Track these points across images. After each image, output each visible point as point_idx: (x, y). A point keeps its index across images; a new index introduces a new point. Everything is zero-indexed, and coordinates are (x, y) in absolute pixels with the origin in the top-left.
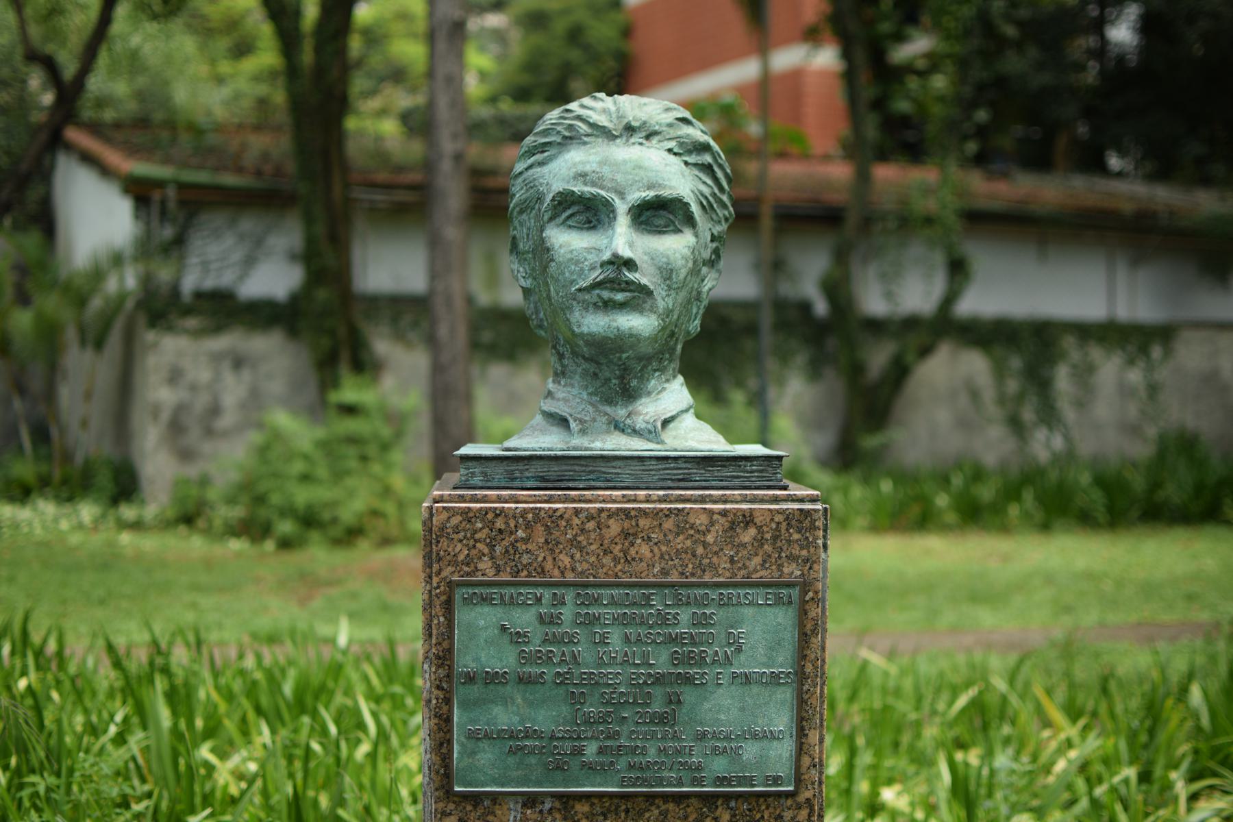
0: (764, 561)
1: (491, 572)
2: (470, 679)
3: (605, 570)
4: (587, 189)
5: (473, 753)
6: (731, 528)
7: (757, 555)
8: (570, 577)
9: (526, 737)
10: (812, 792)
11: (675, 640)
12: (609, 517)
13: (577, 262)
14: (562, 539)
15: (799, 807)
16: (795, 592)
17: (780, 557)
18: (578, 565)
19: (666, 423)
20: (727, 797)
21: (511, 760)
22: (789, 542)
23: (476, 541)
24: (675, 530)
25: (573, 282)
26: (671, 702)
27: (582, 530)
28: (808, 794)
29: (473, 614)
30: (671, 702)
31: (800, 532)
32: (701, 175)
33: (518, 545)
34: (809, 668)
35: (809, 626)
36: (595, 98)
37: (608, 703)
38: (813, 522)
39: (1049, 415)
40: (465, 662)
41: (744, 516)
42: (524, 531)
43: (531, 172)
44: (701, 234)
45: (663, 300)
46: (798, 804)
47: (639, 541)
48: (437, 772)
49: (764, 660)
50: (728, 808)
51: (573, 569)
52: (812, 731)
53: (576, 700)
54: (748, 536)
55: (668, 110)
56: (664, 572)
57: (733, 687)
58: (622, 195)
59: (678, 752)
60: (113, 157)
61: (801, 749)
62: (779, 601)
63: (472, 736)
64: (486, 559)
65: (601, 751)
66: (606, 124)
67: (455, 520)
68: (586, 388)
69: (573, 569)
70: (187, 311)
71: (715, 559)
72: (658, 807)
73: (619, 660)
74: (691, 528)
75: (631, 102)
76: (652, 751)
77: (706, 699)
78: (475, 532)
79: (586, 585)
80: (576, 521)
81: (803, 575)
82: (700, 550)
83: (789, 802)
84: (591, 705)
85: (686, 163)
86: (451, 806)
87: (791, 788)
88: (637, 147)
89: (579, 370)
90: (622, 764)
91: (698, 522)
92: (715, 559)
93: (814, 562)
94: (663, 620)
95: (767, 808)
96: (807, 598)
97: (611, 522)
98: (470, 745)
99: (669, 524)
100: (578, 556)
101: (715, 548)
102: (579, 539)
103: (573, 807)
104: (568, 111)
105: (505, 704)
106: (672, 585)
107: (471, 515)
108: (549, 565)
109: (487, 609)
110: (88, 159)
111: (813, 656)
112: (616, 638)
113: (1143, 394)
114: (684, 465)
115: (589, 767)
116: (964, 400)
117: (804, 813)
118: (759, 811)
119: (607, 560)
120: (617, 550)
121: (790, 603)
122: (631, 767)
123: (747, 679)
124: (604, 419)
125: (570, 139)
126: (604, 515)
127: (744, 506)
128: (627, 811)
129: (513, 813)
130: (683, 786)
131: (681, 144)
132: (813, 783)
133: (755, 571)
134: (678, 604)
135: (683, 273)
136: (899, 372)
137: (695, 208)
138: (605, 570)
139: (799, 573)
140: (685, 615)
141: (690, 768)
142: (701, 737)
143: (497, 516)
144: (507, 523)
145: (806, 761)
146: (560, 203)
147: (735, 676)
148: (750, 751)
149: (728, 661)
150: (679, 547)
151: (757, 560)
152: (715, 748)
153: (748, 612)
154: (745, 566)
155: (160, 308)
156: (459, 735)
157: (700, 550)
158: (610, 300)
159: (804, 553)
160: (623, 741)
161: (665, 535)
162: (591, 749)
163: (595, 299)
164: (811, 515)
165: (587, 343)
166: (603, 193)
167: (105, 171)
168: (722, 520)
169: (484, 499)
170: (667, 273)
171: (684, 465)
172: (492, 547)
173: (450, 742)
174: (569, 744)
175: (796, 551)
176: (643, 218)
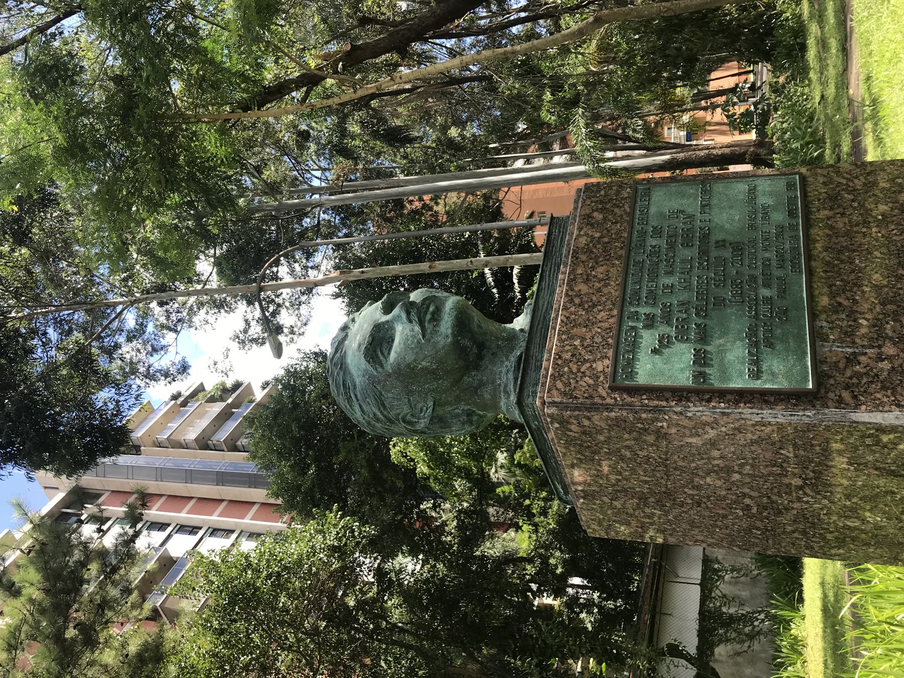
1: (607, 362)
2: (700, 376)
5: (773, 374)
6: (592, 225)
8: (615, 312)
9: (756, 336)
11: (672, 246)
13: (407, 339)
21: (779, 347)
23: (579, 370)
27: (580, 305)
29: (640, 372)
33: (586, 344)
39: (747, 619)
40: (684, 378)
42: (576, 340)
49: (691, 199)
51: (611, 310)
53: (720, 303)
56: (619, 258)
63: (756, 375)
64: (594, 366)
65: (767, 285)
67: (559, 385)
68: (502, 362)
78: (571, 371)
80: (573, 309)
84: (727, 294)
86: (831, 395)
87: (797, 177)
89: (490, 367)
97: (576, 289)
102: (586, 306)
105: (725, 351)
107: (557, 374)
113: (735, 574)
116: (739, 659)
121: (649, 189)
134: (642, 245)
140: (652, 242)
142: (752, 227)
143: (560, 357)
144: (567, 352)
146: (373, 358)
149: (691, 217)
151: (617, 210)
153: (653, 210)
159: (614, 188)
162: (765, 292)
163: (431, 326)
168: (585, 229)
172: (586, 361)
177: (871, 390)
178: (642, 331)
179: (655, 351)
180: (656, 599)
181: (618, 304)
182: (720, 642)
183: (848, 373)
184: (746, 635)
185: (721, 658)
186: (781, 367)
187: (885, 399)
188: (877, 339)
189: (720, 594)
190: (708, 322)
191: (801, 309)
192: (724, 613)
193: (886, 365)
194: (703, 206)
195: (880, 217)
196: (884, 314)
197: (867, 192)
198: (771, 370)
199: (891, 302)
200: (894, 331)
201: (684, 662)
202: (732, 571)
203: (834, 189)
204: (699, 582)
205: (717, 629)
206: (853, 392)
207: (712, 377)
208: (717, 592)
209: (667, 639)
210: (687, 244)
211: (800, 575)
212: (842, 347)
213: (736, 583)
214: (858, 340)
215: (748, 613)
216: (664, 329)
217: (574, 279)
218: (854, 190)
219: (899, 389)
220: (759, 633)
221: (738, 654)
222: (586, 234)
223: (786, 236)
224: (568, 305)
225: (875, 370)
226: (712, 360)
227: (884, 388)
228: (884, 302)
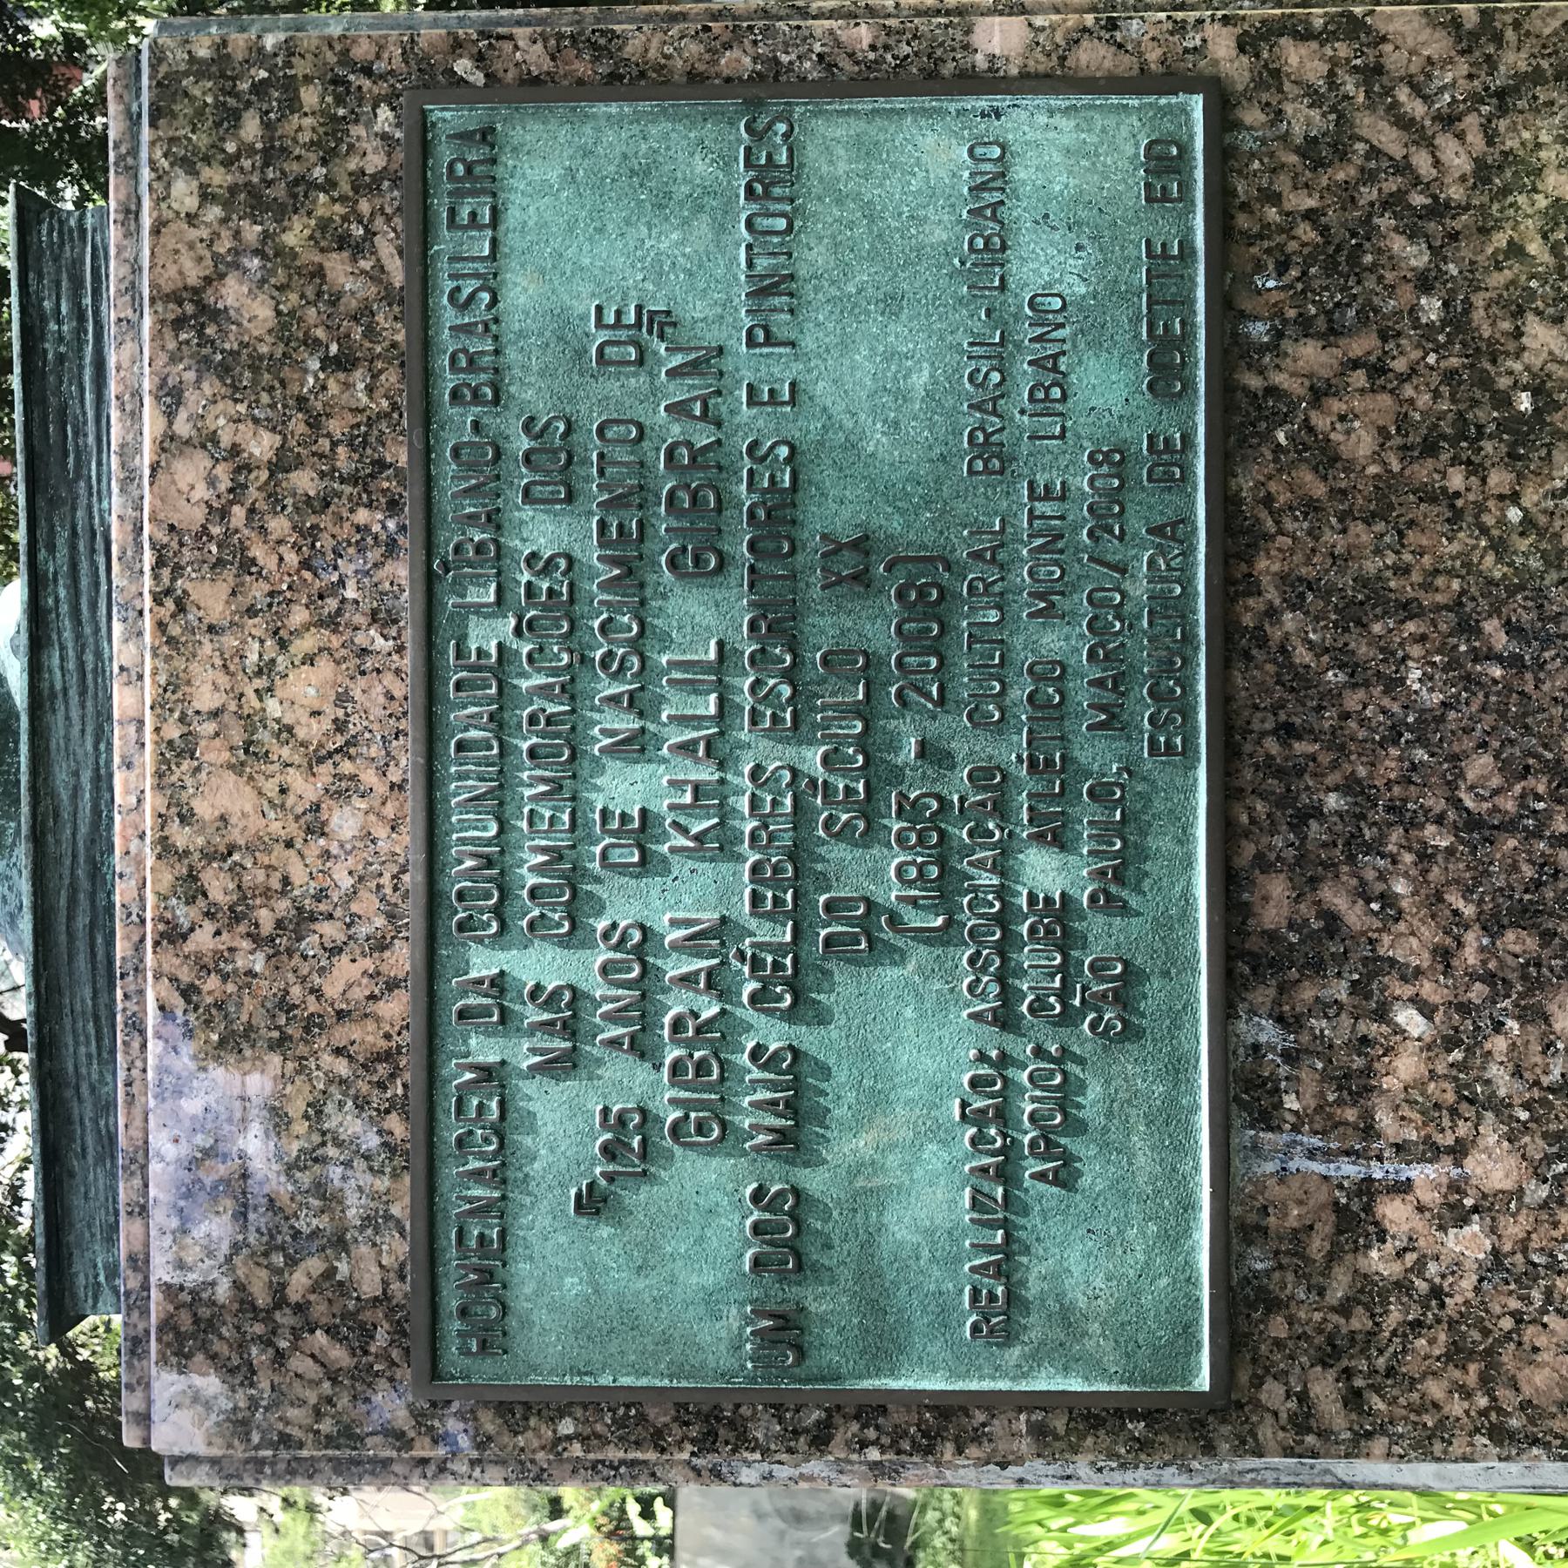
0: (343, 242)
2: (785, 1330)
3: (381, 832)
5: (1067, 1317)
6: (224, 371)
7: (319, 273)
8: (402, 958)
9: (1003, 1116)
10: (1210, 30)
12: (186, 818)
15: (1270, 77)
16: (447, 117)
17: (329, 184)
18: (363, 930)
20: (1230, 351)
21: (1093, 1176)
22: (272, 152)
24: (229, 574)
26: (861, 578)
27: (235, 917)
28: (1222, 44)
29: (541, 1317)
30: (861, 578)
34: (738, 61)
37: (869, 810)
38: (198, 69)
41: (179, 324)
46: (1259, 84)
47: (273, 707)
48: (1143, 1446)
49: (703, 227)
50: (1274, 347)
51: (380, 945)
52: (978, 39)
57: (808, 343)
59: (1053, 541)
62: (483, 180)
64: (343, 1268)
69: (380, 945)
71: (336, 427)
72: (1272, 613)
73: (706, 774)
74: (224, 514)
76: (1053, 641)
77: (851, 446)
80: (203, 940)
81: (391, 99)
82: (304, 481)
83: (1252, 116)
84: (876, 874)
86: (1272, 1393)
87: (1197, 104)
90: (1098, 755)
91: (202, 492)
92: (336, 427)
93: (345, 57)
95: (1275, 198)
96: (478, 78)
98: (1035, 1328)
100: (331, 931)
101: (297, 425)
102: (267, 927)
103: (1272, 936)
105: (877, 1197)
106: (430, 583)
108: (365, 1036)
109: (524, 1274)
111: (693, 48)
112: (622, 788)
114: (62, 552)
117: (1297, 57)
118: (1287, 230)
119: (345, 822)
120: (306, 789)
121: (486, 135)
123: (773, 288)
126: (181, 837)
128: (1287, 732)
129: (1298, 1163)
130: (1187, 520)
132: (1180, 28)
133: (378, 274)
138: (381, 832)
139: (384, 113)
141: (1115, 496)
142: (993, 457)
145: (1093, 56)
147: (763, 337)
148: (1046, 265)
149: (705, 363)
150: (292, 559)
151: (338, 268)
152: (1042, 404)
153: (522, 293)
154: (364, 314)
156: (998, 1371)
157: (304, 481)
159: (310, 96)
160: (1011, 751)
161: (251, 612)
162: (1044, 872)
164: (175, 76)
171: (62, 552)
175: (303, 127)
177: (1411, 1366)
178: (529, 1087)
179: (592, 1203)
181: (413, 913)
183: (1339, 1288)
186: (1099, 1282)
187: (1457, 1407)
188: (1454, 1112)
190: (808, 1038)
191: (1176, 966)
194: (764, 289)
195: (1525, 402)
196: (1489, 978)
197: (1484, 231)
198: (1059, 1298)
199: (1525, 916)
200: (1517, 1073)
206: (1348, 1374)
207: (830, 1334)
212: (1328, 1155)
214: (1384, 1119)
216: (628, 1082)
218: (1439, 209)
219: (1507, 1355)
223: (1138, 527)
224: (184, 914)
225: (1432, 1268)
226: (828, 1246)
227: (1457, 1354)
228: (1495, 915)
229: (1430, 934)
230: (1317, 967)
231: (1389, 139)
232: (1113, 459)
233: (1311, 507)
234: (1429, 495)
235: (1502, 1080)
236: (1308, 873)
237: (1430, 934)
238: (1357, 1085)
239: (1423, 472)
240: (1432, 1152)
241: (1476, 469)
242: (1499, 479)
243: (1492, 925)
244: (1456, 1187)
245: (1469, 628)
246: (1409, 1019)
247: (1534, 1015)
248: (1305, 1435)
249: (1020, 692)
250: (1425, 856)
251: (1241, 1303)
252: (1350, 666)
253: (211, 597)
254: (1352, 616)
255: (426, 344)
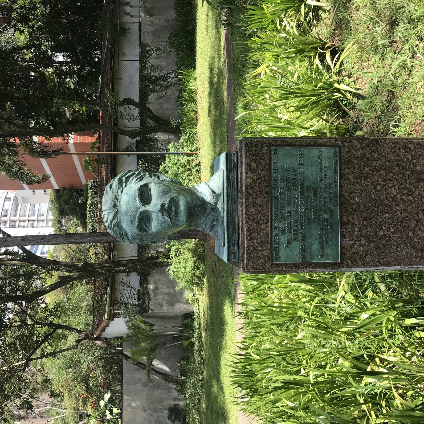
0: (262, 159)
1: (268, 251)
2: (303, 257)
4: (136, 220)
5: (328, 256)
8: (269, 224)
9: (322, 238)
11: (289, 188)
13: (162, 223)
14: (256, 227)
15: (344, 146)
19: (214, 192)
20: (341, 170)
21: (330, 243)
22: (256, 151)
25: (168, 224)
28: (340, 143)
30: (310, 190)
31: (252, 147)
32: (130, 181)
34: (298, 143)
35: (284, 143)
36: (103, 217)
37: (310, 211)
39: (165, 78)
40: (298, 259)
43: (130, 238)
44: (150, 181)
45: (174, 194)
48: (334, 267)
49: (295, 158)
51: (266, 223)
53: (309, 222)
54: (254, 165)
55: (107, 193)
56: (267, 193)
58: (138, 208)
59: (326, 187)
60: (103, 324)
61: (325, 145)
62: (276, 154)
63: (322, 256)
65: (326, 213)
66: (113, 214)
67: (251, 263)
69: (266, 223)
70: (144, 302)
71: (262, 176)
75: (105, 205)
79: (271, 219)
82: (259, 181)
83: (342, 149)
85: (126, 186)
88: (121, 203)
90: (330, 206)
92: (262, 176)
94: (282, 193)
99: (251, 191)
101: (258, 176)
104: (108, 226)
105: (311, 245)
108: (265, 231)
110: (103, 330)
112: (288, 209)
115: (331, 217)
116: (161, 100)
119: (263, 212)
120: (259, 209)
122: (331, 203)
124: (212, 212)
125: (118, 225)
127: (244, 166)
128: (346, 204)
131: (119, 188)
133: (266, 162)
135: (164, 187)
136: (154, 117)
137: (142, 183)
140: (281, 185)
142: (321, 179)
143: (249, 249)
144: (251, 246)
145: (329, 143)
146: (141, 229)
148: (325, 163)
151: (262, 161)
153: (279, 164)
155: (143, 309)
157: (259, 181)
158: (175, 212)
159: (259, 145)
162: (326, 216)
163: (174, 217)
165: (189, 219)
166: (138, 215)
167: (107, 326)
168: (249, 173)
169: (243, 253)
170: (165, 193)
172: (259, 251)
173: (324, 263)
174: (324, 224)
175: (259, 148)
176: (146, 201)
177: (357, 259)
180: (113, 71)
182: (152, 92)
184: (164, 87)
185: (152, 101)
189: (150, 65)
192: (153, 76)
193: (361, 249)
194: (301, 164)
199: (365, 220)
201: (134, 107)
202: (156, 50)
203: (350, 156)
204: (138, 59)
205: (149, 86)
208: (149, 64)
209: (123, 96)
210: (295, 188)
211: (195, 56)
213: (159, 58)
215: (165, 74)
217: (248, 205)
218: (358, 158)
220: (171, 85)
221: (161, 98)
222: (250, 177)
227: (361, 258)
229: (358, 221)
230: (348, 224)
231: (353, 151)
232: (331, 179)
233: (347, 184)
234: (357, 183)
235: (364, 234)
236: (348, 216)
237: (358, 221)
238: (352, 235)
239: (357, 181)
240: (358, 241)
241: (361, 181)
242: (363, 181)
243: (363, 221)
244: (360, 244)
245: (361, 195)
246: (356, 229)
247: (366, 228)
248: (348, 266)
249: (323, 200)
250: (357, 215)
251: (343, 254)
252: (351, 198)
253: (251, 191)
254: (351, 193)
255: (270, 169)
